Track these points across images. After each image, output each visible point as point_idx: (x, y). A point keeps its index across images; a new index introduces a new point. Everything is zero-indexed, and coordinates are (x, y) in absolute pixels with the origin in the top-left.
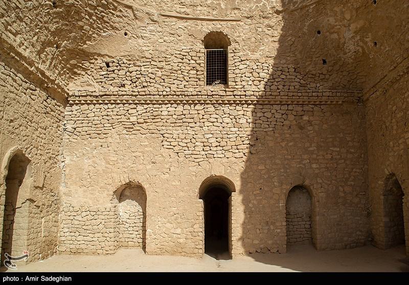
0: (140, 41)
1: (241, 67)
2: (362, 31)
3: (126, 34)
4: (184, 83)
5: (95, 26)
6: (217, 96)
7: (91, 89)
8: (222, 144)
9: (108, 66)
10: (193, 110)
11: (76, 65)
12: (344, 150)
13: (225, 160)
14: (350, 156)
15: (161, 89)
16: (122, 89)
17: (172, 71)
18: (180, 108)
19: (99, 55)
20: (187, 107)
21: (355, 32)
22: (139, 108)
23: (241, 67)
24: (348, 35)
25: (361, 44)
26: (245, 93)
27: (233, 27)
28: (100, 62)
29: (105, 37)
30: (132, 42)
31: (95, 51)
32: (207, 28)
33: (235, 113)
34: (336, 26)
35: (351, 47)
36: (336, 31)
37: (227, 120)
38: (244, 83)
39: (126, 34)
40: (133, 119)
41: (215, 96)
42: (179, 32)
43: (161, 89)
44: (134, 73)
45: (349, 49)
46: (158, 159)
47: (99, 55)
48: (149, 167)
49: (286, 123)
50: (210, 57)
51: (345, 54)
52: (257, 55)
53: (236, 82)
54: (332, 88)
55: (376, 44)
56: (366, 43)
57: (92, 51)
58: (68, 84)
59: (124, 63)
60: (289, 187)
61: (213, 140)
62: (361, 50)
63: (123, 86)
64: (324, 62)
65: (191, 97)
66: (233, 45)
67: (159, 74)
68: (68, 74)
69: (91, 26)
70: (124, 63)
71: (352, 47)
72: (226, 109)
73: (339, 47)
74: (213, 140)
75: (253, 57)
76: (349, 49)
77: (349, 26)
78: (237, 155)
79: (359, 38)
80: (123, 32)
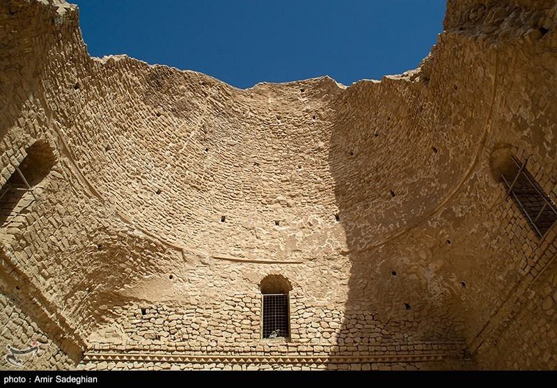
0: (187, 285)
2: (444, 271)
3: (171, 277)
4: (235, 335)
5: (138, 268)
6: (277, 353)
7: (117, 341)
9: (144, 312)
11: (105, 310)
15: (205, 342)
16: (157, 342)
19: (136, 300)
21: (436, 272)
24: (429, 275)
25: (446, 284)
26: (312, 349)
27: (294, 270)
28: (135, 308)
29: (148, 280)
30: (178, 286)
31: (132, 295)
32: (265, 271)
34: (412, 266)
35: (436, 288)
36: (413, 271)
38: (310, 335)
39: (171, 277)
41: (274, 353)
42: (233, 275)
43: (205, 342)
45: (434, 291)
47: (136, 300)
50: (267, 302)
51: (431, 296)
52: (324, 301)
53: (300, 334)
54: (425, 339)
55: (464, 284)
56: (452, 284)
57: (129, 295)
58: (89, 334)
59: (163, 310)
62: (448, 291)
63: (158, 338)
64: (408, 306)
65: (243, 354)
66: (295, 290)
67: (205, 323)
68: (93, 321)
69: (134, 268)
70: (163, 310)
71: (437, 289)
73: (422, 289)
75: (321, 303)
76: (434, 291)
77: (427, 265)
79: (442, 279)
80: (168, 275)
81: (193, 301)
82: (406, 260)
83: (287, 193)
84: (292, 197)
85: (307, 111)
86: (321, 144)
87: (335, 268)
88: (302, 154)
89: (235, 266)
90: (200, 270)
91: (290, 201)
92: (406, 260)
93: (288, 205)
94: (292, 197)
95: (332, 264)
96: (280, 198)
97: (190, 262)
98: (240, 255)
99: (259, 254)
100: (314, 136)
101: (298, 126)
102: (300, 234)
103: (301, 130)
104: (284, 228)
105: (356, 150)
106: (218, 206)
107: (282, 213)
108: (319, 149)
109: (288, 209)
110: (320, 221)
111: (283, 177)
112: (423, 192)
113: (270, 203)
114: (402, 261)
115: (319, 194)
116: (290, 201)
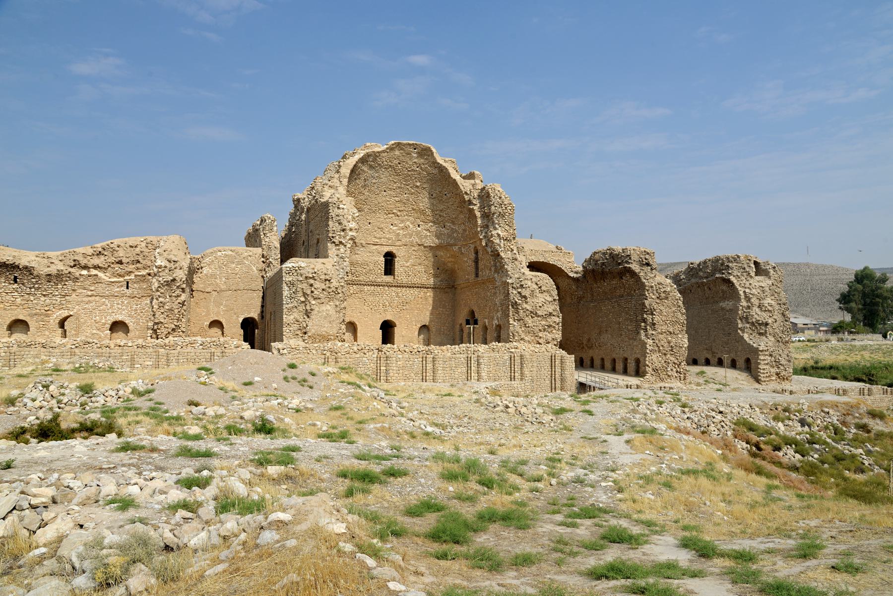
0: (356, 255)
1: (401, 269)
4: (375, 276)
8: (391, 305)
10: (378, 288)
12: (444, 310)
13: (392, 313)
14: (447, 313)
15: (365, 278)
17: (370, 270)
18: (373, 287)
20: (376, 287)
22: (354, 286)
23: (401, 269)
27: (398, 250)
32: (386, 249)
33: (397, 291)
37: (394, 294)
40: (351, 292)
43: (365, 278)
44: (353, 271)
46: (363, 311)
48: (358, 314)
49: (420, 296)
50: (386, 261)
54: (441, 281)
60: (419, 326)
61: (387, 303)
64: (438, 269)
67: (364, 271)
72: (393, 289)
74: (387, 303)
75: (406, 265)
78: (398, 310)
81: (360, 262)
82: (442, 254)
83: (398, 209)
84: (400, 211)
85: (415, 162)
86: (418, 184)
87: (414, 250)
88: (408, 187)
89: (375, 247)
92: (442, 254)
93: (398, 215)
94: (400, 211)
95: (413, 248)
96: (395, 211)
97: (358, 246)
98: (377, 242)
99: (383, 241)
100: (416, 178)
101: (409, 171)
102: (401, 232)
103: (410, 173)
104: (395, 228)
105: (434, 195)
106: (368, 217)
108: (417, 187)
109: (397, 217)
110: (411, 226)
112: (455, 235)
113: (389, 214)
115: (413, 212)
116: (399, 213)
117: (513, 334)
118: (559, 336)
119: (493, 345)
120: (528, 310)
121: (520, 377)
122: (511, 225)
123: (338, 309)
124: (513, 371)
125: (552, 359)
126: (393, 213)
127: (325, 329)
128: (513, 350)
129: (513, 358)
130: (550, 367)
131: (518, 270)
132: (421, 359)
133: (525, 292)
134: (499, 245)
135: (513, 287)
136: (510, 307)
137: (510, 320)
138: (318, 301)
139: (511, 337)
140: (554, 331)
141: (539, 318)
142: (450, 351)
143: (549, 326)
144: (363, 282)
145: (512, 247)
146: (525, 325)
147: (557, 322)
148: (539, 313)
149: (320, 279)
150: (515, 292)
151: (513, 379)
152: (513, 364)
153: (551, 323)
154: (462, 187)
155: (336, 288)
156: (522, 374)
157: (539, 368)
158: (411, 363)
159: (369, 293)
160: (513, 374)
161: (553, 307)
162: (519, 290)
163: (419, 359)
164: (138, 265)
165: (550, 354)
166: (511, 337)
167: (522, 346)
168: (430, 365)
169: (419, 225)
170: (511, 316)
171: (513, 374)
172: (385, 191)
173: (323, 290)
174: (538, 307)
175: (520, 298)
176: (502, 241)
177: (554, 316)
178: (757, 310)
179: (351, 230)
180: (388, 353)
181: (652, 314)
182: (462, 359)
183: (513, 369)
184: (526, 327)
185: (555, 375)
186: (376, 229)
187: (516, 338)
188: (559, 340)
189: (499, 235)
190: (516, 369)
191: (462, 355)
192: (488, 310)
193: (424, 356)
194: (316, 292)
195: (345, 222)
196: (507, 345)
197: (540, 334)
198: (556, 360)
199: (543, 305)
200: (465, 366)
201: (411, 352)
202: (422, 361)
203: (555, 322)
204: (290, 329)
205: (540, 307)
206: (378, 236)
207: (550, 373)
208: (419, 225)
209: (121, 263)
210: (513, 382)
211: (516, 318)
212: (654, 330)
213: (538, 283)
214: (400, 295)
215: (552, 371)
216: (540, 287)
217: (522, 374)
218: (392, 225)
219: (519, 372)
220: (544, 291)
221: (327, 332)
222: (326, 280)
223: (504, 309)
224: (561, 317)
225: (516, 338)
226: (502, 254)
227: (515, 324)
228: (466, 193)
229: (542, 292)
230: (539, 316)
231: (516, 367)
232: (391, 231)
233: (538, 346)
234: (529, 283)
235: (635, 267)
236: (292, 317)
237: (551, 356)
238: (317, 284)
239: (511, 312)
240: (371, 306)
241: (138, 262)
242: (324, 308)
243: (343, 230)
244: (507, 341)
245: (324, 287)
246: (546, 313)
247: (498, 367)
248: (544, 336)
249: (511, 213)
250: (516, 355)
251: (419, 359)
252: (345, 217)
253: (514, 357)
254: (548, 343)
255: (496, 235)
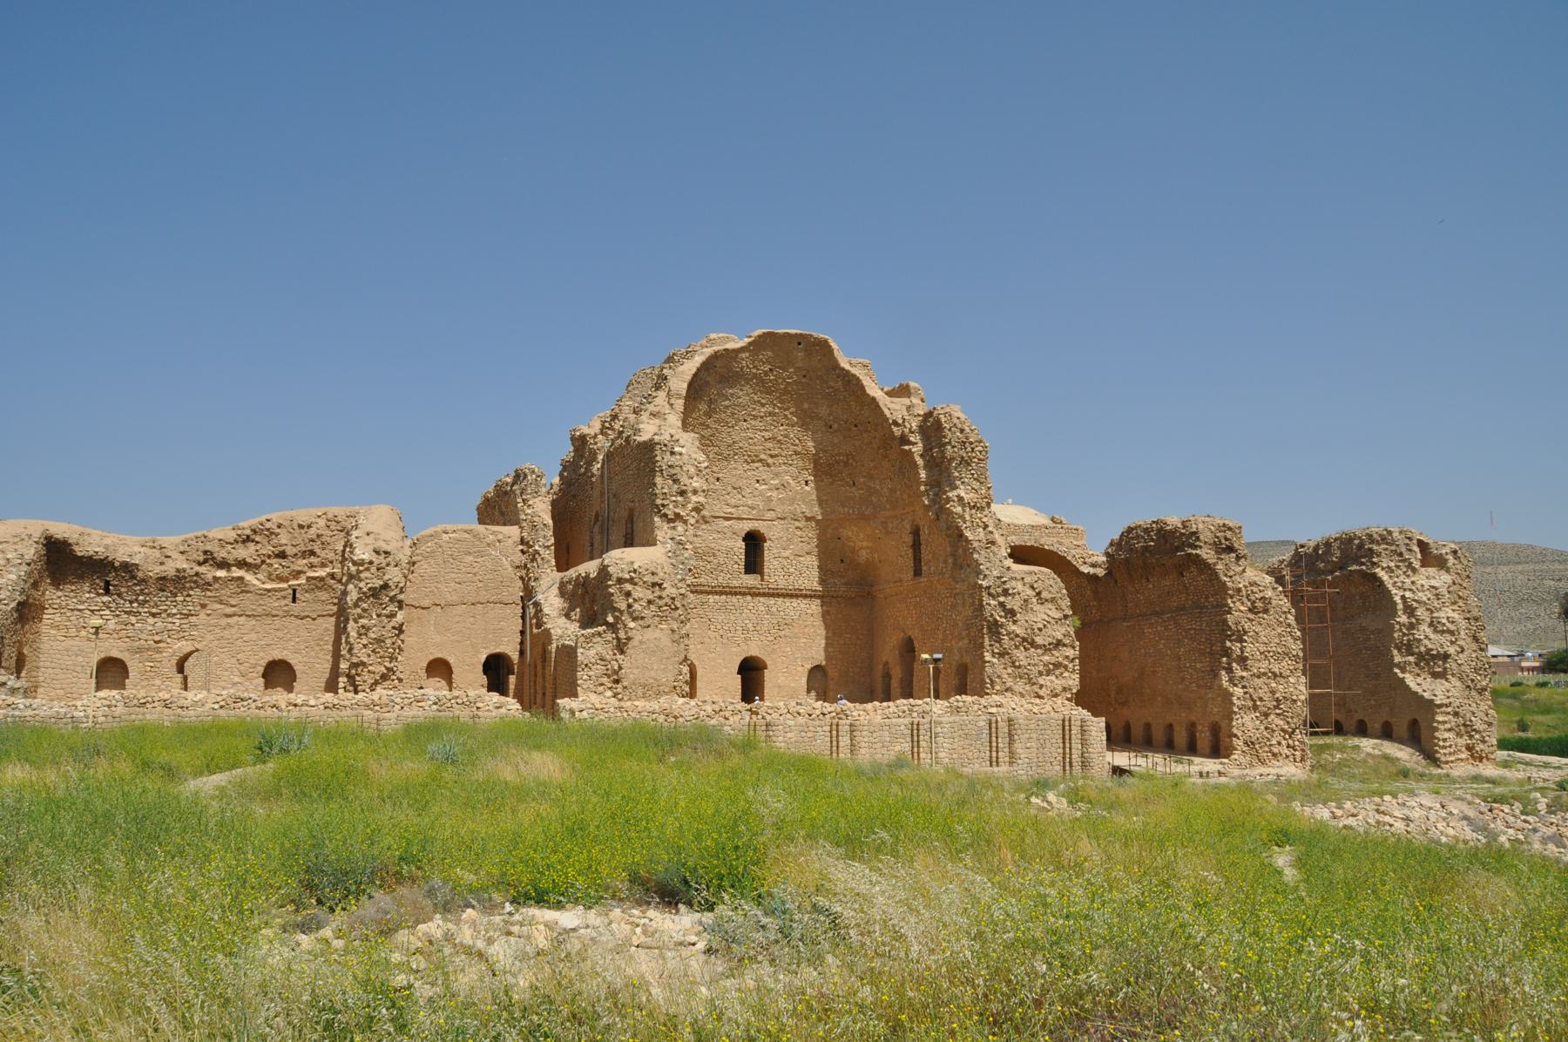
4: (729, 576)
8: (758, 628)
10: (734, 599)
13: (760, 643)
14: (859, 642)
17: (719, 565)
18: (724, 597)
32: (747, 526)
35: (863, 553)
42: (726, 530)
46: (707, 640)
48: (699, 646)
49: (809, 611)
61: (750, 625)
64: (842, 561)
66: (768, 543)
67: (709, 566)
72: (761, 599)
74: (750, 625)
78: (769, 639)
81: (700, 551)
82: (850, 533)
83: (768, 452)
84: (772, 456)
89: (727, 523)
90: (704, 527)
91: (770, 461)
92: (850, 533)
93: (768, 465)
94: (772, 456)
95: (797, 524)
96: (763, 456)
98: (730, 513)
99: (743, 512)
102: (775, 494)
104: (764, 487)
107: (763, 473)
111: (767, 434)
113: (753, 462)
114: (846, 532)
115: (794, 457)
116: (770, 461)
117: (991, 680)
118: (1073, 681)
119: (958, 701)
120: (1017, 636)
121: (1007, 759)
122: (982, 480)
123: (677, 637)
124: (994, 749)
125: (1065, 725)
126: (761, 461)
127: (653, 674)
128: (994, 710)
129: (994, 725)
130: (1060, 741)
131: (998, 562)
132: (828, 728)
133: (1012, 603)
134: (962, 517)
135: (989, 594)
136: (985, 631)
137: (986, 654)
138: (640, 622)
139: (988, 686)
140: (1066, 674)
141: (1039, 651)
142: (879, 712)
143: (1057, 665)
144: (706, 588)
145: (985, 520)
146: (1013, 663)
147: (1071, 657)
148: (1039, 640)
149: (645, 582)
150: (993, 602)
151: (994, 764)
152: (994, 735)
153: (1060, 659)
154: (887, 412)
155: (673, 599)
156: (1012, 754)
157: (1042, 741)
158: (810, 735)
159: (717, 607)
160: (994, 754)
161: (1063, 631)
162: (1002, 599)
163: (824, 728)
164: (313, 559)
165: (1061, 717)
166: (988, 686)
167: (1010, 701)
168: (845, 739)
169: (807, 482)
170: (988, 648)
171: (994, 754)
172: (745, 421)
173: (650, 602)
174: (1036, 630)
175: (1003, 614)
176: (968, 509)
177: (1065, 645)
178: (1429, 631)
179: (695, 492)
180: (768, 717)
181: (1241, 641)
182: (903, 727)
183: (994, 744)
184: (1015, 667)
185: (1071, 754)
186: (730, 489)
187: (998, 688)
188: (1074, 691)
189: (960, 499)
190: (1001, 745)
191: (901, 720)
192: (941, 637)
193: (835, 721)
194: (636, 606)
195: (684, 479)
196: (983, 701)
197: (1041, 681)
198: (1073, 727)
199: (1045, 626)
200: (909, 739)
201: (810, 715)
202: (831, 732)
203: (1067, 657)
204: (591, 673)
205: (1040, 630)
206: (733, 502)
207: (1061, 751)
208: (807, 482)
209: (282, 555)
210: (996, 769)
211: (996, 651)
212: (1246, 669)
213: (1035, 585)
214: (774, 609)
215: (1064, 748)
216: (1039, 594)
217: (1012, 754)
218: (758, 481)
219: (1007, 750)
220: (1047, 600)
221: (656, 680)
222: (654, 585)
223: (972, 634)
224: (1077, 648)
225: (998, 688)
226: (968, 534)
227: (995, 660)
228: (895, 423)
229: (1042, 601)
230: (1037, 647)
231: (1000, 740)
232: (756, 493)
233: (1037, 701)
234: (1020, 586)
235: (1207, 554)
236: (592, 652)
237: (1064, 721)
238: (639, 592)
239: (987, 640)
240: (721, 632)
241: (312, 553)
242: (650, 634)
243: (682, 493)
244: (981, 692)
245: (651, 597)
246: (1050, 640)
247: (967, 742)
248: (1049, 684)
249: (982, 457)
250: (999, 719)
251: (824, 728)
252: (685, 469)
253: (997, 722)
254: (1056, 695)
255: (956, 499)
